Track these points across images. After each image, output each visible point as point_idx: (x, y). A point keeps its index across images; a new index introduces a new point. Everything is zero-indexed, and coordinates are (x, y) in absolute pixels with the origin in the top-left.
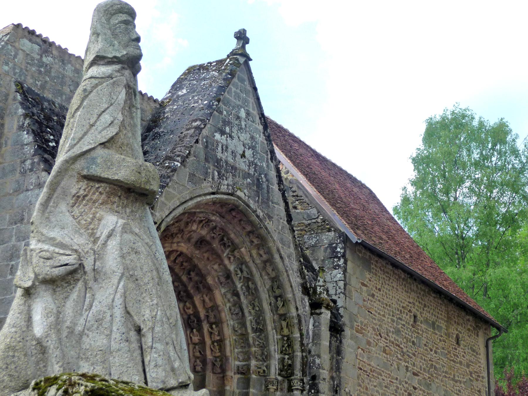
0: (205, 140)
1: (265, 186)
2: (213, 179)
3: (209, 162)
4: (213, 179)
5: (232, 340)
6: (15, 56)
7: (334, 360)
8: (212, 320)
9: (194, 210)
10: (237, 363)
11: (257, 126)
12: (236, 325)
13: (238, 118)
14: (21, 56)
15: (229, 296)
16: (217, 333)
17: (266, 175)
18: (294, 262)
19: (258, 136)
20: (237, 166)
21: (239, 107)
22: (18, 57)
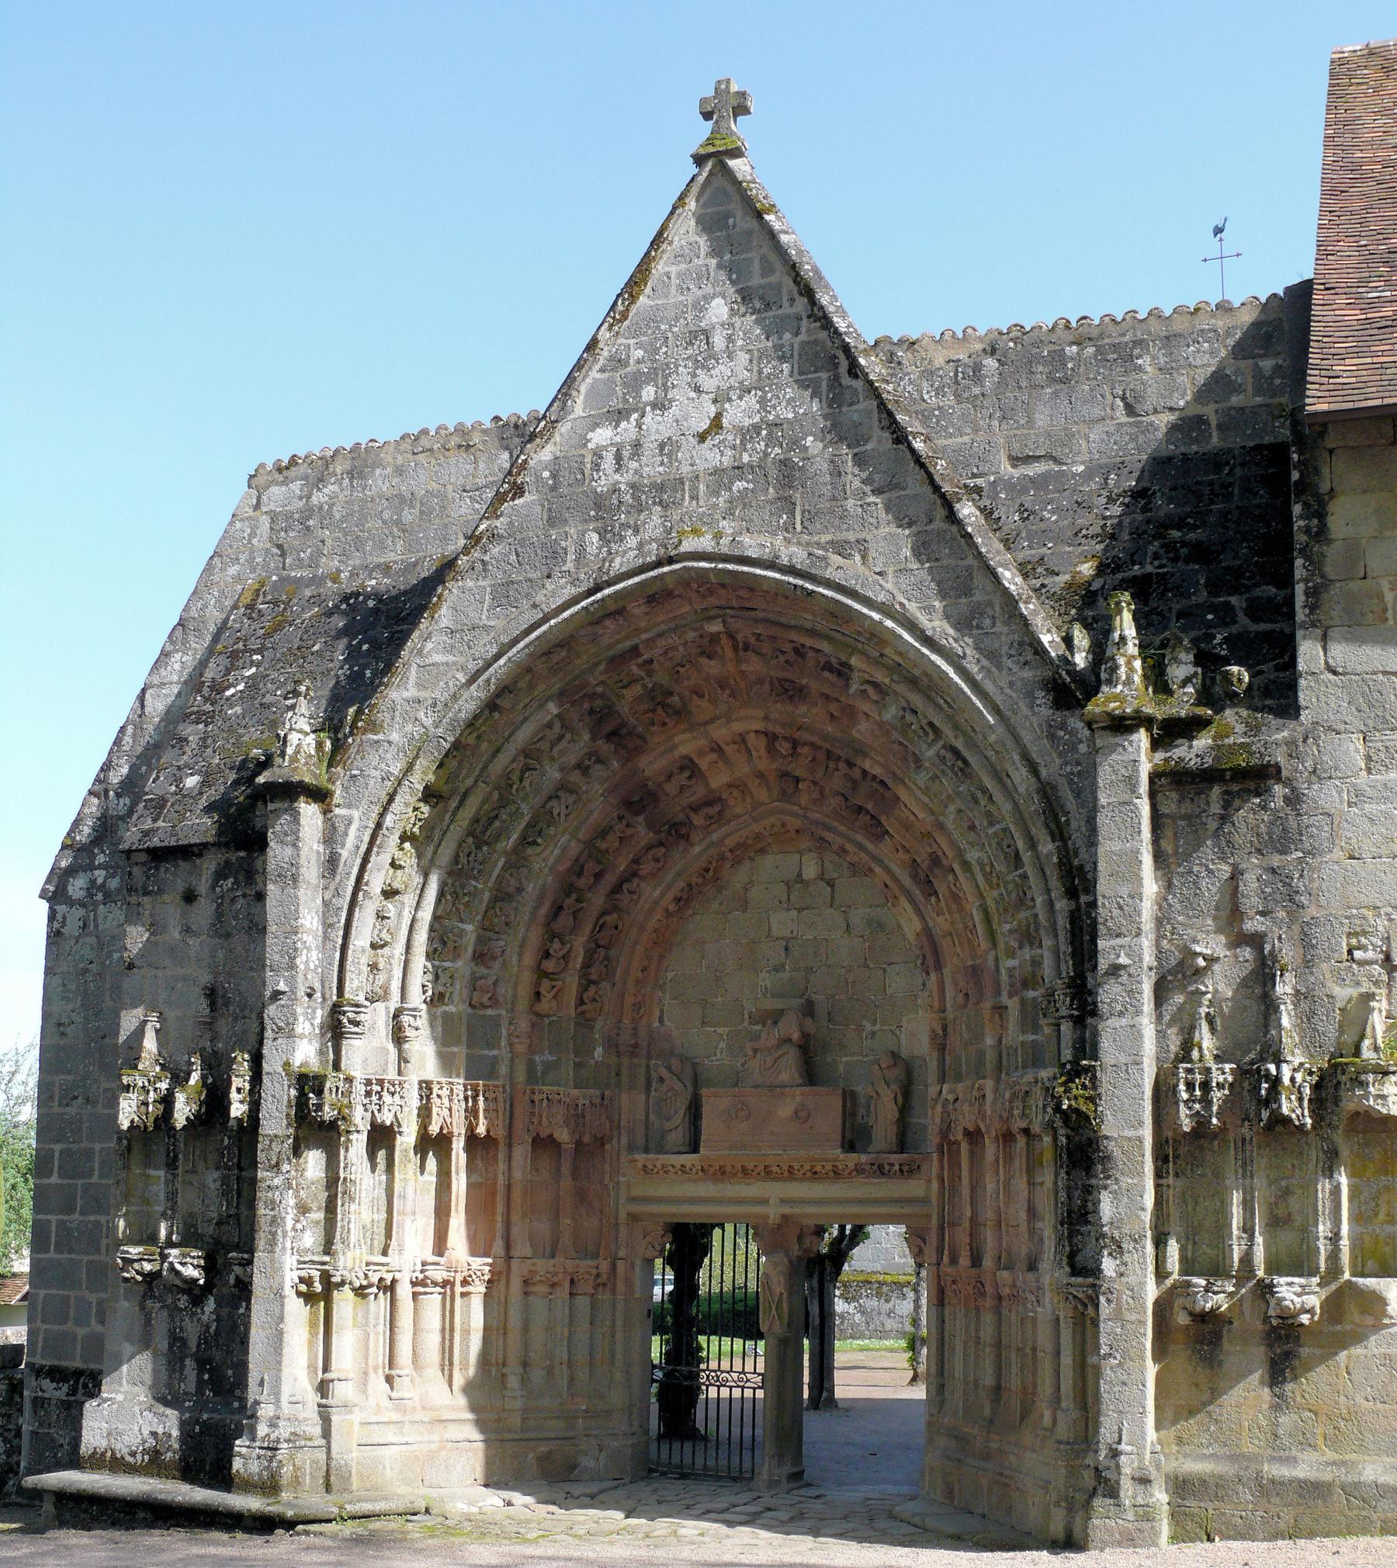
0: (546, 474)
5: (990, 903)
6: (252, 535)
9: (628, 644)
18: (1000, 628)
19: (787, 336)
21: (700, 307)
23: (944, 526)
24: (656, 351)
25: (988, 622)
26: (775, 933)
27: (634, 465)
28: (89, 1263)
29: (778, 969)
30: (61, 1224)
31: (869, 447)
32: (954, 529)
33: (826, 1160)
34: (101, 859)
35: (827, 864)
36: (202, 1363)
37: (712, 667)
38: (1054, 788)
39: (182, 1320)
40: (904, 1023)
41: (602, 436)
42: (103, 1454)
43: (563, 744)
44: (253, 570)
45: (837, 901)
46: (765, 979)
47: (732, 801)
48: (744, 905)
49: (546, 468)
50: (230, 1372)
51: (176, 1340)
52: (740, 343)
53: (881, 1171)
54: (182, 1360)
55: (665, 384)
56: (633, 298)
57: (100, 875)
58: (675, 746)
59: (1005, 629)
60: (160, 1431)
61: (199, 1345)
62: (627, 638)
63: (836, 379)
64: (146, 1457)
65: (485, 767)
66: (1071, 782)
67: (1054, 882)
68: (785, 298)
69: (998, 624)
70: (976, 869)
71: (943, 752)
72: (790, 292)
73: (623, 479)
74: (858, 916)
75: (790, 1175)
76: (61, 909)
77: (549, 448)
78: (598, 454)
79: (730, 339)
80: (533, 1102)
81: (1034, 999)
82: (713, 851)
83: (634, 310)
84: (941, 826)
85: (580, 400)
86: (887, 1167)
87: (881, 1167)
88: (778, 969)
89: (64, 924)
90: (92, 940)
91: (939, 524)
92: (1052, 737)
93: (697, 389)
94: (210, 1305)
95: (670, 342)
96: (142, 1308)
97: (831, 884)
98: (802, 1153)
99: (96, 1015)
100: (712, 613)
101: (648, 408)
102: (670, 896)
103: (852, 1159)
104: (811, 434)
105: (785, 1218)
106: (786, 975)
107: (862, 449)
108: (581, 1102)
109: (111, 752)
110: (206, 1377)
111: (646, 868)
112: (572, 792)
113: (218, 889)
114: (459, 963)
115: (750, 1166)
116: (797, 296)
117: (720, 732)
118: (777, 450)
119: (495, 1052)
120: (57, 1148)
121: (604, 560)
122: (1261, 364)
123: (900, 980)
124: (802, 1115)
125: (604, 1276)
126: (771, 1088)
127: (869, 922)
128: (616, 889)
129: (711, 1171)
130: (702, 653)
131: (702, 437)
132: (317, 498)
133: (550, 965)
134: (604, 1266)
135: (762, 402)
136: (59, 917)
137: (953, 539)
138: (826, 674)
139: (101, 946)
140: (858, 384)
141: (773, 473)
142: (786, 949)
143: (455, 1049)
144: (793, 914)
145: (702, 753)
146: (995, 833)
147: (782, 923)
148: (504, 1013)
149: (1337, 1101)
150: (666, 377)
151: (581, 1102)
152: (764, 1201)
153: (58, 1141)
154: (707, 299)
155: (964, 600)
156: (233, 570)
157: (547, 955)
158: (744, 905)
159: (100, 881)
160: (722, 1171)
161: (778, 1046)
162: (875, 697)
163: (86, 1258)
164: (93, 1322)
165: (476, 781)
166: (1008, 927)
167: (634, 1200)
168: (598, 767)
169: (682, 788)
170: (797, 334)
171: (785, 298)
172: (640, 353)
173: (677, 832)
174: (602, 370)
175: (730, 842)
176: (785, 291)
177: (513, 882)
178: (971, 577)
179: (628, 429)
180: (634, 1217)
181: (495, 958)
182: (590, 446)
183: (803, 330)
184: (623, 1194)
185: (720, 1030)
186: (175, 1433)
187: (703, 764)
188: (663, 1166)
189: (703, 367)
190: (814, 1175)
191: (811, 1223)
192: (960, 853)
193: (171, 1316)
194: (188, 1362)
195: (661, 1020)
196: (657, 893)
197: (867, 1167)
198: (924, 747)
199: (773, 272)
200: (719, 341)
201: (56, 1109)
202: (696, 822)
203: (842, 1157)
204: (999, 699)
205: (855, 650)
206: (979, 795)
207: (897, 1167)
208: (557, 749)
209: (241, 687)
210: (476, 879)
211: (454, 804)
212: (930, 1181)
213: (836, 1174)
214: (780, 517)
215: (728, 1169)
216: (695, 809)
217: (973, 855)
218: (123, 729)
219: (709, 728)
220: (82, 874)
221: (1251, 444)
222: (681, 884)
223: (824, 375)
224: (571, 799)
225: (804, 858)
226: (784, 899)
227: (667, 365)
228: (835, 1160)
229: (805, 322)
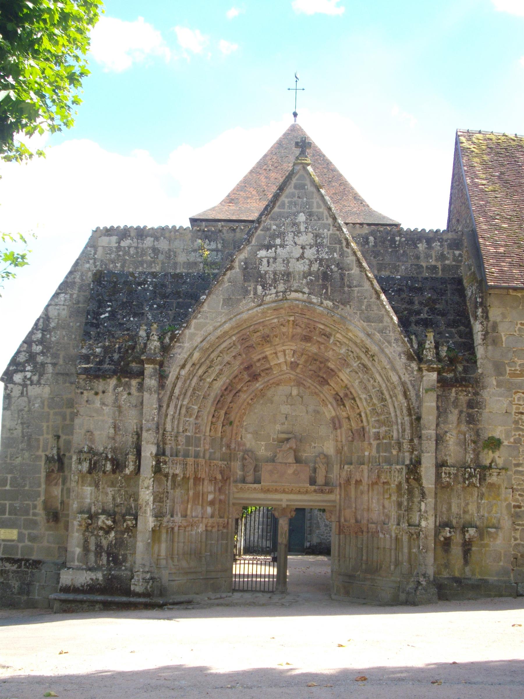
0: (243, 263)
1: (337, 276)
2: (255, 293)
3: (250, 281)
4: (255, 293)
6: (95, 253)
7: (464, 415)
8: (351, 396)
9: (262, 320)
10: (374, 430)
11: (325, 221)
12: (368, 398)
13: (295, 224)
14: (100, 250)
15: (353, 374)
16: (356, 407)
17: (338, 265)
18: (391, 334)
19: (326, 230)
20: (291, 270)
21: (296, 214)
22: (98, 253)
23: (375, 300)
24: (281, 227)
25: (388, 332)
26: (282, 412)
27: (274, 265)
28: (25, 520)
29: (283, 424)
30: (10, 504)
31: (352, 272)
32: (378, 302)
34: (28, 368)
35: (301, 391)
36: (109, 554)
37: (284, 329)
38: (406, 383)
39: (101, 540)
40: (325, 444)
41: (262, 253)
42: (70, 587)
43: (232, 349)
44: (96, 267)
46: (278, 427)
47: (274, 370)
48: (272, 403)
49: (242, 261)
50: (121, 557)
51: (99, 546)
52: (310, 230)
53: (322, 492)
54: (101, 553)
55: (284, 239)
56: (273, 207)
57: (29, 375)
58: (265, 352)
59: (393, 335)
60: (94, 577)
61: (108, 548)
62: (262, 319)
63: (341, 248)
64: (88, 588)
65: (209, 355)
66: (411, 383)
67: (405, 411)
68: (325, 218)
69: (391, 333)
70: (364, 400)
71: (360, 365)
72: (326, 216)
73: (271, 269)
74: (311, 408)
75: (291, 492)
76: (10, 386)
77: (243, 254)
78: (261, 259)
79: (306, 228)
80: (210, 466)
81: (386, 443)
82: (266, 384)
83: (273, 211)
84: (353, 386)
85: (254, 240)
87: (322, 490)
88: (283, 424)
89: (11, 392)
90: (26, 399)
91: (373, 300)
92: (406, 369)
93: (295, 243)
94: (113, 534)
95: (286, 225)
96: (84, 535)
97: (302, 397)
99: (28, 427)
100: (291, 314)
101: (278, 247)
102: (250, 398)
103: (313, 488)
104: (334, 265)
105: (287, 505)
106: (285, 426)
107: (350, 272)
108: (223, 466)
109: (33, 328)
110: (111, 559)
111: (245, 389)
112: (229, 364)
113: (116, 391)
114: (191, 419)
115: (278, 488)
116: (329, 217)
117: (280, 348)
118: (322, 268)
119: (199, 449)
120: (9, 476)
121: (264, 296)
122: (455, 252)
123: (324, 430)
124: (296, 473)
125: (226, 524)
126: (286, 463)
127: (314, 411)
128: (235, 395)
130: (282, 325)
131: (298, 260)
132: (123, 244)
133: (214, 420)
134: (226, 520)
135: (318, 251)
136: (9, 388)
137: (378, 305)
138: (323, 336)
139: (29, 402)
140: (349, 251)
141: (321, 276)
142: (286, 417)
143: (190, 448)
144: (289, 406)
145: (271, 354)
146: (375, 391)
147: (285, 409)
148: (202, 435)
149: (485, 480)
150: (284, 237)
151: (223, 466)
152: (281, 500)
153: (9, 473)
154: (298, 213)
155: (381, 324)
156: (87, 266)
157: (213, 416)
159: (28, 376)
160: (268, 490)
162: (339, 346)
163: (23, 518)
164: (26, 541)
165: (205, 360)
166: (373, 419)
167: (235, 498)
168: (240, 356)
169: (262, 364)
170: (329, 230)
171: (325, 218)
172: (274, 227)
173: (255, 377)
174: (262, 230)
175: (271, 382)
176: (325, 215)
177: (208, 392)
178: (383, 317)
179: (271, 253)
180: (234, 504)
181: (199, 417)
182: (258, 256)
183: (331, 230)
184: (231, 496)
185: (263, 443)
186: (101, 578)
187: (270, 358)
189: (297, 236)
190: (299, 492)
191: (295, 507)
192: (359, 395)
193: (96, 538)
194: (103, 554)
195: (241, 438)
196: (245, 397)
198: (353, 363)
199: (320, 207)
200: (302, 228)
201: (8, 461)
202: (262, 375)
203: (310, 487)
204: (390, 356)
205: (338, 332)
206: (371, 379)
207: (327, 491)
208: (230, 350)
209: (107, 315)
210: (198, 391)
211: (197, 367)
212: (336, 495)
213: (307, 492)
214: (323, 290)
215: (271, 489)
216: (263, 371)
217: (363, 396)
218: (38, 320)
219: (276, 347)
220: (20, 373)
221: (451, 277)
222: (254, 394)
223: (338, 246)
224: (229, 366)
226: (286, 401)
227: (285, 232)
229: (331, 227)
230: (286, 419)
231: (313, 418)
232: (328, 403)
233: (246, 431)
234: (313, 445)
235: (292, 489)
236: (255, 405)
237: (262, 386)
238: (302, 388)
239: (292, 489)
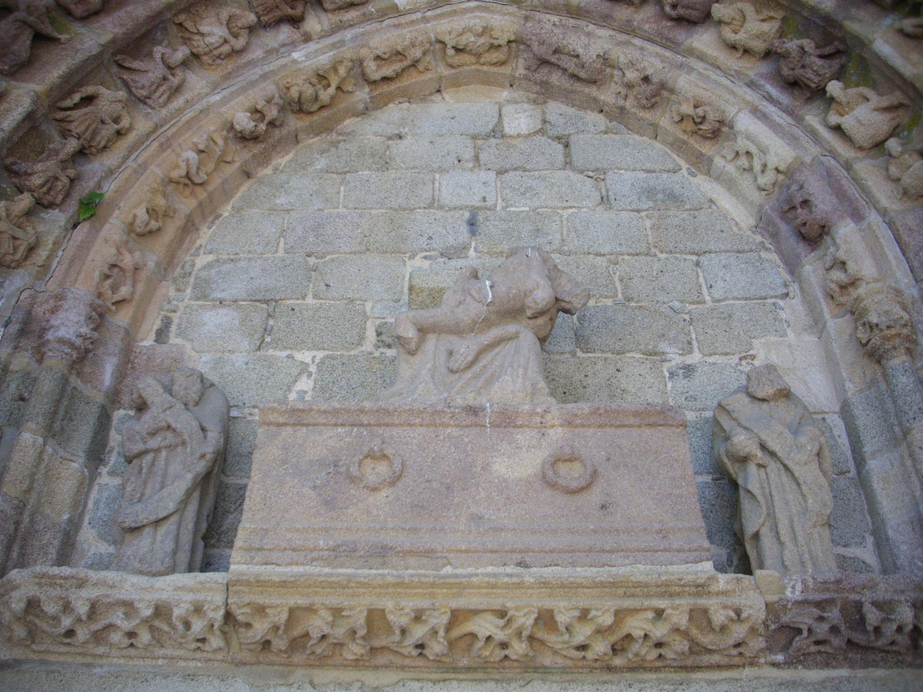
26: (446, 197)
33: (667, 590)
45: (578, 160)
86: (873, 616)
98: (584, 573)
129: (260, 628)
142: (472, 223)
158: (385, 164)
161: (486, 323)
185: (305, 356)
188: (94, 610)
195: (161, 335)
197: (805, 620)
225: (508, 109)
228: (701, 589)
230: (473, 233)
231: (648, 223)
232: (731, 111)
233: (204, 297)
234: (676, 359)
235: (546, 619)
236: (283, 177)
237: (324, 60)
238: (556, 110)
239: (546, 619)
